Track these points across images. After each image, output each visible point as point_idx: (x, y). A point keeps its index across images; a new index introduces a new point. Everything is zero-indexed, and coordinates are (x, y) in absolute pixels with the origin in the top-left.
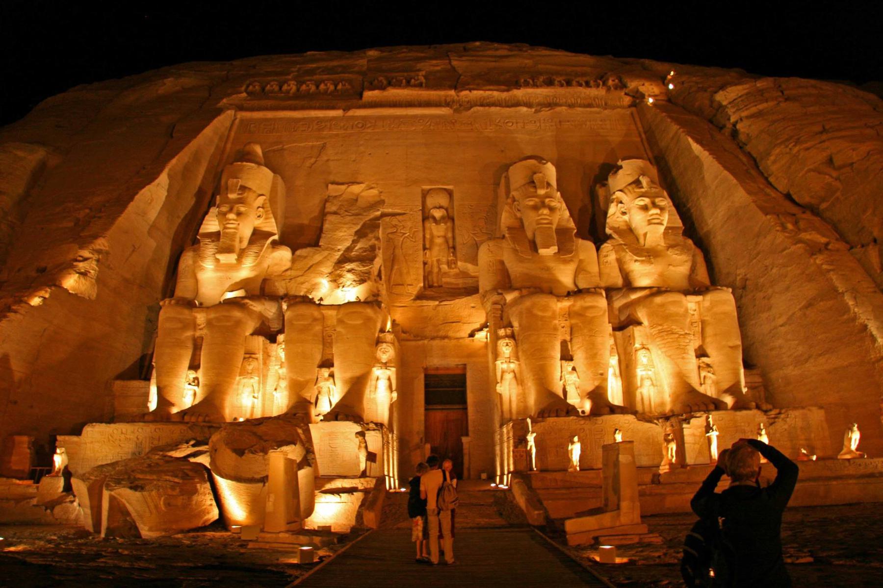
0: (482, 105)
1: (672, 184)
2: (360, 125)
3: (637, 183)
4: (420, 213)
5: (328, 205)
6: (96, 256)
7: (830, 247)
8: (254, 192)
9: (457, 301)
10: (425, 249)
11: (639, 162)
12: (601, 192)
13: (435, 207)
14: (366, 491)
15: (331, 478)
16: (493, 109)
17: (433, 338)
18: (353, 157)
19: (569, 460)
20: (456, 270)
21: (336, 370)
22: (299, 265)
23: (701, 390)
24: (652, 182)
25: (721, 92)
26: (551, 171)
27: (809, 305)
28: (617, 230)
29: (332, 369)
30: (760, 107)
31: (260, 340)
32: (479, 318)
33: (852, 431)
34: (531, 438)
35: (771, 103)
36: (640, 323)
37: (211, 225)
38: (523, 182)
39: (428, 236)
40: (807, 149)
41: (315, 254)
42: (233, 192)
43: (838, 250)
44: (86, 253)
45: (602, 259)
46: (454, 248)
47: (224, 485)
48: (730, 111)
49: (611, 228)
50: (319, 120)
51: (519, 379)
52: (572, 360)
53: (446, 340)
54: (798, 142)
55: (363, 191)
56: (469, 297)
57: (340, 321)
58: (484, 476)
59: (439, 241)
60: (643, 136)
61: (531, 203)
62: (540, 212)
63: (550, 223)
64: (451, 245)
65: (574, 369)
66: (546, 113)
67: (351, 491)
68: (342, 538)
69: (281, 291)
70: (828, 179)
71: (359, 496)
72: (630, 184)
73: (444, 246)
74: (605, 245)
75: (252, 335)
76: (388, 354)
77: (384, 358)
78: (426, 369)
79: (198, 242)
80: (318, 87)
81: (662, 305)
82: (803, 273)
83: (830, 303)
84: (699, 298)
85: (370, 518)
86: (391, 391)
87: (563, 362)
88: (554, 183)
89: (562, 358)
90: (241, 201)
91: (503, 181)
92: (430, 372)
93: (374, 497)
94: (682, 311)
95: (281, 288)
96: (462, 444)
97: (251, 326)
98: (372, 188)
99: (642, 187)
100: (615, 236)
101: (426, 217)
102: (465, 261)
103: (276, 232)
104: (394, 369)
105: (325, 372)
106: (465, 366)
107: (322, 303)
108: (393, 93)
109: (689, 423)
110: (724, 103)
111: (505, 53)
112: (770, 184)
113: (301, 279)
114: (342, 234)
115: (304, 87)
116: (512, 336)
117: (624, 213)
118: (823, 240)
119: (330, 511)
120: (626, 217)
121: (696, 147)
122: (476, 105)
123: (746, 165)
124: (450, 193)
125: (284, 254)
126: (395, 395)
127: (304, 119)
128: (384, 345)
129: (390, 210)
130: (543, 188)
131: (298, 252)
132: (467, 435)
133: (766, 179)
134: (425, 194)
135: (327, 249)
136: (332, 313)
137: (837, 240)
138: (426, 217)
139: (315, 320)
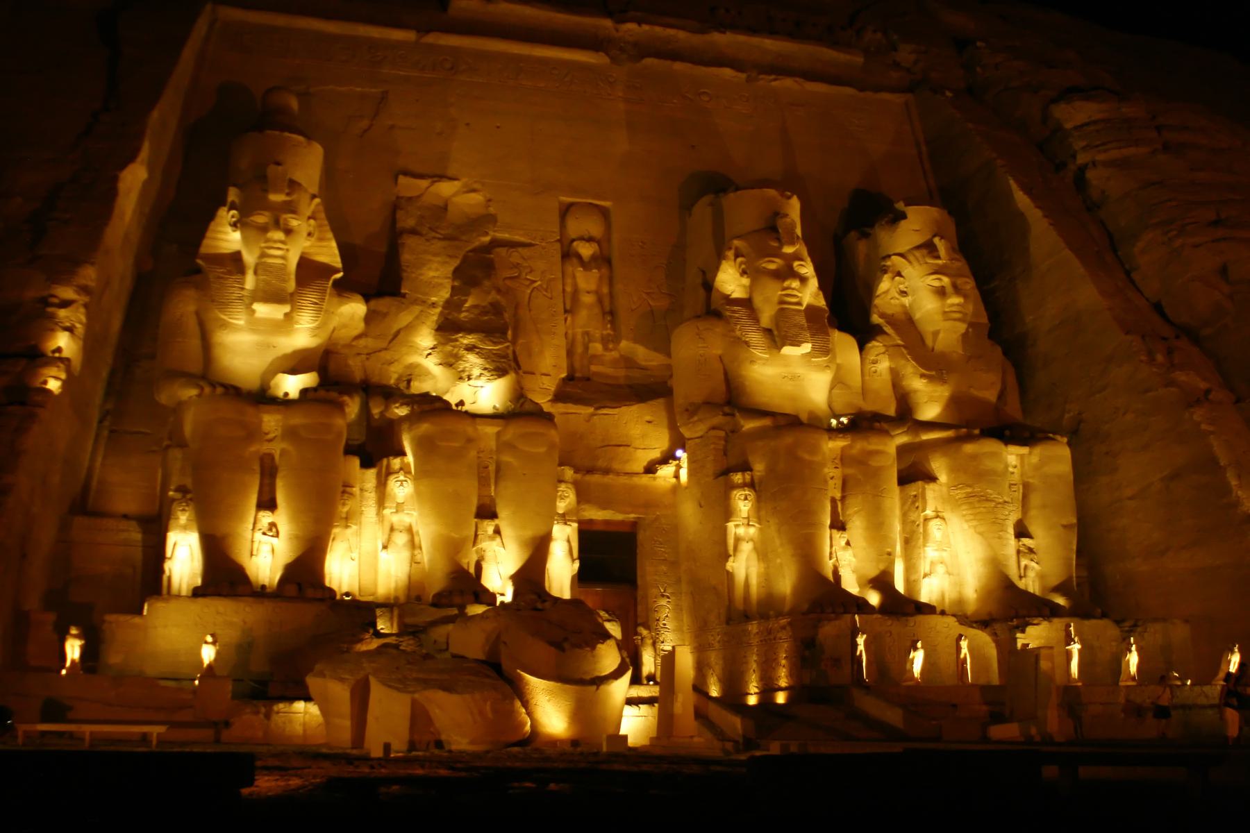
0: (659, 55)
1: (985, 260)
4: (558, 246)
5: (400, 214)
6: (84, 299)
7: (1211, 397)
9: (624, 409)
10: (566, 311)
13: (582, 239)
16: (678, 66)
20: (615, 354)
21: (503, 522)
23: (1021, 584)
26: (794, 208)
28: (891, 320)
29: (497, 521)
33: (1233, 652)
36: (933, 479)
39: (569, 289)
40: (1196, 246)
42: (278, 191)
44: (67, 293)
45: (868, 366)
46: (612, 313)
48: (1078, 144)
49: (882, 316)
51: (762, 552)
55: (455, 194)
56: (642, 405)
59: (588, 299)
60: (924, 149)
61: (772, 267)
62: (786, 284)
63: (799, 304)
64: (607, 309)
65: (848, 543)
69: (358, 376)
72: (918, 247)
73: (597, 310)
74: (874, 343)
76: (568, 500)
77: (561, 506)
81: (974, 457)
84: (1024, 450)
86: (573, 560)
87: (834, 531)
89: (832, 527)
98: (474, 191)
99: (938, 257)
100: (888, 329)
101: (568, 254)
103: (339, 265)
105: (489, 527)
109: (1023, 631)
110: (1068, 126)
114: (432, 274)
116: (751, 485)
118: (1203, 385)
120: (906, 301)
121: (1022, 200)
122: (649, 56)
124: (604, 213)
125: (355, 309)
129: (506, 236)
131: (373, 303)
136: (490, 430)
138: (568, 254)
139: (470, 440)
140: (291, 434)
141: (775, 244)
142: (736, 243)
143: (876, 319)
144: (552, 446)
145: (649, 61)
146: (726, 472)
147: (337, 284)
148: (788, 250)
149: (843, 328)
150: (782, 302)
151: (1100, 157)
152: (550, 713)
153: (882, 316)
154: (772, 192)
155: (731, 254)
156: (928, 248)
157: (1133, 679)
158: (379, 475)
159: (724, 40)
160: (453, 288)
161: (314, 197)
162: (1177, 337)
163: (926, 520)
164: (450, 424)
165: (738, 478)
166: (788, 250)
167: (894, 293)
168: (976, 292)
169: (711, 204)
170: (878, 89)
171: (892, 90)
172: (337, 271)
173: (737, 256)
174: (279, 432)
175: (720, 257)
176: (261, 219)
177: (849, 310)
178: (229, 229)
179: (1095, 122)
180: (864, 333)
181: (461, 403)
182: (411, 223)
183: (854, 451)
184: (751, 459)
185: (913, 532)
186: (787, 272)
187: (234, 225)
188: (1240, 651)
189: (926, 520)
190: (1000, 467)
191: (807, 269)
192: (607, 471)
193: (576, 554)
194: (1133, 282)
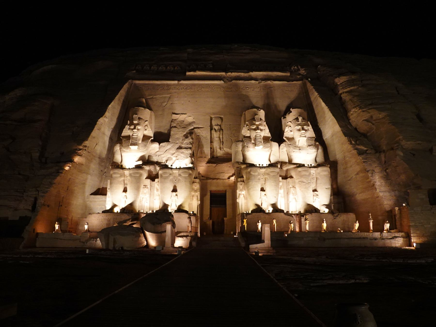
2: (185, 88)
3: (297, 119)
8: (144, 120)
11: (299, 110)
12: (283, 121)
14: (191, 237)
15: (181, 232)
17: (213, 179)
18: (182, 102)
19: (258, 228)
22: (161, 150)
24: (303, 118)
25: (338, 78)
26: (262, 114)
27: (357, 174)
30: (351, 88)
31: (149, 180)
32: (232, 172)
34: (245, 221)
35: (355, 87)
37: (126, 132)
38: (251, 118)
42: (135, 121)
43: (370, 153)
47: (147, 233)
49: (285, 137)
50: (168, 85)
52: (264, 191)
54: (360, 108)
57: (180, 175)
58: (232, 233)
60: (305, 94)
62: (257, 131)
63: (260, 136)
64: (221, 141)
67: (186, 236)
68: (186, 249)
70: (370, 124)
71: (189, 238)
73: (219, 142)
75: (146, 178)
78: (211, 191)
79: (121, 140)
80: (166, 68)
81: (300, 172)
82: (356, 161)
83: (363, 174)
85: (194, 244)
88: (263, 119)
89: (261, 190)
90: (138, 124)
91: (243, 115)
92: (212, 192)
93: (194, 238)
94: (307, 174)
95: (155, 159)
96: (224, 220)
97: (145, 175)
102: (227, 148)
104: (199, 193)
106: (226, 191)
107: (172, 167)
108: (198, 73)
111: (247, 51)
115: (160, 68)
117: (291, 131)
118: (365, 149)
119: (179, 242)
120: (292, 133)
121: (323, 104)
124: (222, 119)
125: (156, 146)
126: (199, 202)
127: (161, 84)
128: (196, 184)
129: (197, 126)
130: (258, 121)
131: (161, 144)
132: (226, 217)
133: (349, 120)
134: (211, 119)
135: (172, 143)
137: (371, 149)
139: (170, 174)
140: (130, 175)
145: (233, 81)
148: (257, 123)
149: (274, 141)
150: (256, 136)
151: (345, 90)
152: (152, 240)
154: (255, 110)
155: (245, 125)
157: (325, 230)
159: (254, 74)
162: (361, 137)
166: (257, 123)
167: (289, 131)
168: (312, 129)
170: (293, 81)
172: (152, 137)
173: (247, 126)
176: (132, 127)
177: (277, 136)
179: (345, 82)
182: (175, 125)
185: (288, 191)
188: (359, 222)
192: (218, 179)
193: (199, 199)
194: (350, 123)
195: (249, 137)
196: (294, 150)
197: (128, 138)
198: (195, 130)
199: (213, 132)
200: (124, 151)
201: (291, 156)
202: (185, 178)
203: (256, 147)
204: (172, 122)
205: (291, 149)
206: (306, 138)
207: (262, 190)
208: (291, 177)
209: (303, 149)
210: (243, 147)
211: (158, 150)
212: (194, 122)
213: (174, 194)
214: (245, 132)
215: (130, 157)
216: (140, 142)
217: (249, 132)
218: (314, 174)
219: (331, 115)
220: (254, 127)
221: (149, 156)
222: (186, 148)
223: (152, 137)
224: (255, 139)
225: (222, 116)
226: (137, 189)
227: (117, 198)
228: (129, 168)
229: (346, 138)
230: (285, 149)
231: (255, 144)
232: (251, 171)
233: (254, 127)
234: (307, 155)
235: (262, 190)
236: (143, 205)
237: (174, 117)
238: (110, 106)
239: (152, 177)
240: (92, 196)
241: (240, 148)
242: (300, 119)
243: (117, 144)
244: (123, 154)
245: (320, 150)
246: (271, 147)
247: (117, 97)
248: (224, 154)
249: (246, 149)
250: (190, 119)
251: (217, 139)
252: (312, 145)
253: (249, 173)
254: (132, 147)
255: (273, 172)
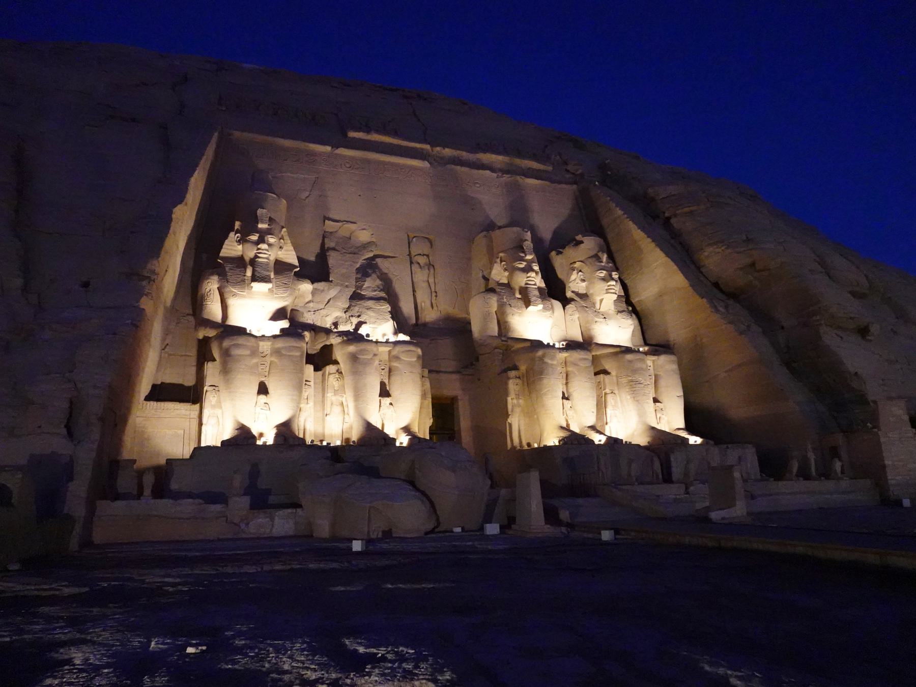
5: (326, 240)
22: (317, 298)
23: (659, 427)
37: (232, 248)
41: (329, 289)
42: (262, 223)
49: (573, 292)
53: (441, 374)
61: (522, 266)
66: (506, 178)
81: (630, 362)
90: (269, 232)
112: (702, 273)
113: (323, 312)
114: (345, 271)
117: (583, 281)
120: (584, 284)
123: (684, 255)
125: (306, 287)
131: (316, 285)
135: (337, 285)
136: (384, 349)
139: (375, 355)
140: (277, 352)
141: (523, 255)
142: (501, 255)
143: (569, 294)
144: (419, 357)
146: (506, 371)
147: (296, 274)
148: (529, 257)
150: (527, 284)
153: (573, 292)
155: (498, 260)
156: (597, 257)
158: (323, 375)
160: (356, 278)
161: (283, 227)
163: (606, 394)
164: (362, 346)
165: (512, 373)
167: (578, 281)
169: (485, 236)
171: (566, 183)
172: (296, 267)
173: (501, 261)
174: (269, 352)
175: (491, 263)
176: (255, 237)
177: (555, 291)
178: (236, 244)
180: (566, 302)
181: (368, 335)
182: (332, 245)
183: (571, 359)
184: (517, 364)
186: (528, 269)
187: (239, 242)
189: (606, 394)
190: (644, 366)
191: (536, 268)
195: (508, 286)
196: (597, 319)
197: (240, 262)
198: (378, 260)
199: (415, 267)
200: (235, 295)
201: (589, 330)
202: (410, 364)
203: (531, 308)
204: (324, 237)
205: (591, 316)
206: (615, 297)
207: (564, 397)
208: (606, 372)
209: (610, 319)
210: (502, 307)
211: (310, 297)
212: (370, 243)
213: (386, 401)
214: (499, 274)
215: (253, 309)
216: (272, 276)
217: (507, 274)
218: (651, 368)
219: (662, 255)
220: (522, 265)
221: (292, 310)
222: (371, 299)
223: (296, 267)
224: (524, 291)
225: (431, 237)
226: (300, 385)
227: (241, 410)
228: (263, 336)
229: (705, 300)
230: (577, 315)
231: (527, 303)
232: (544, 356)
233: (522, 265)
234: (617, 331)
235: (564, 397)
236: (302, 428)
237: (330, 226)
238: (193, 180)
239: (321, 360)
240: (153, 404)
241: (495, 307)
242: (605, 257)
243: (212, 274)
244: (232, 302)
245: (636, 322)
246: (552, 308)
247: (202, 162)
248: (439, 320)
249: (509, 310)
250: (364, 236)
251: (425, 285)
252: (623, 311)
253: (541, 359)
254: (257, 286)
255: (585, 359)
